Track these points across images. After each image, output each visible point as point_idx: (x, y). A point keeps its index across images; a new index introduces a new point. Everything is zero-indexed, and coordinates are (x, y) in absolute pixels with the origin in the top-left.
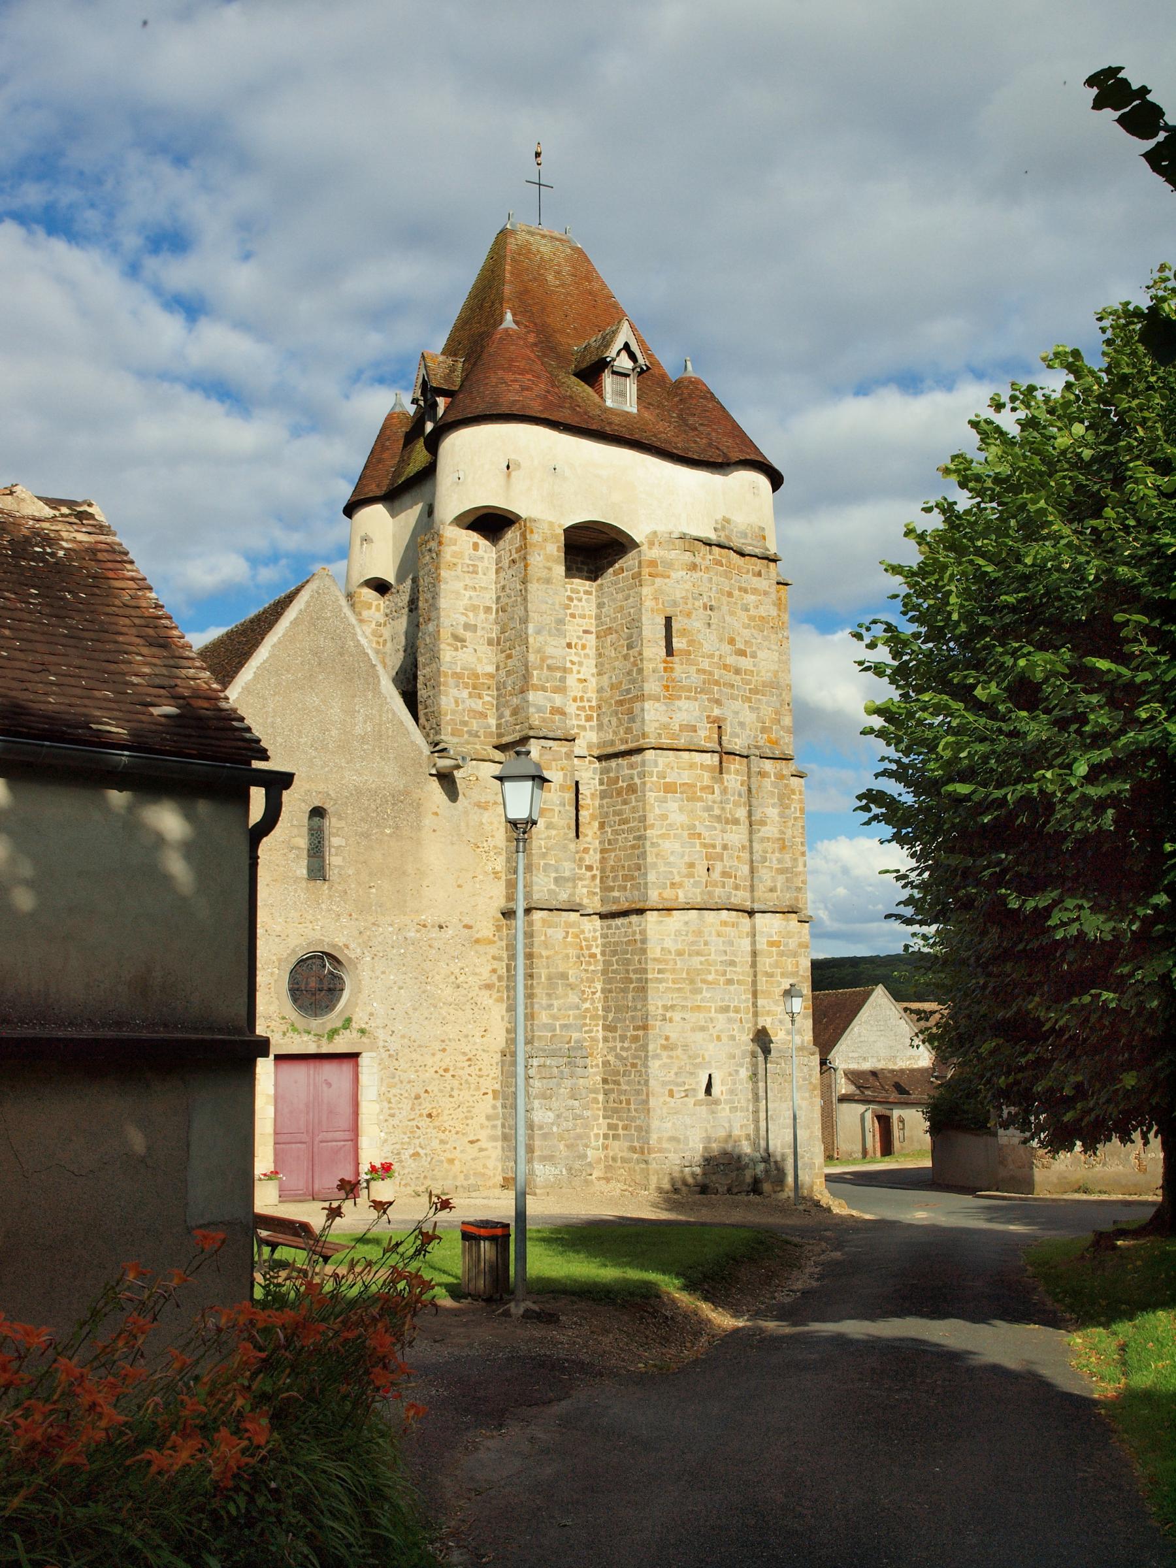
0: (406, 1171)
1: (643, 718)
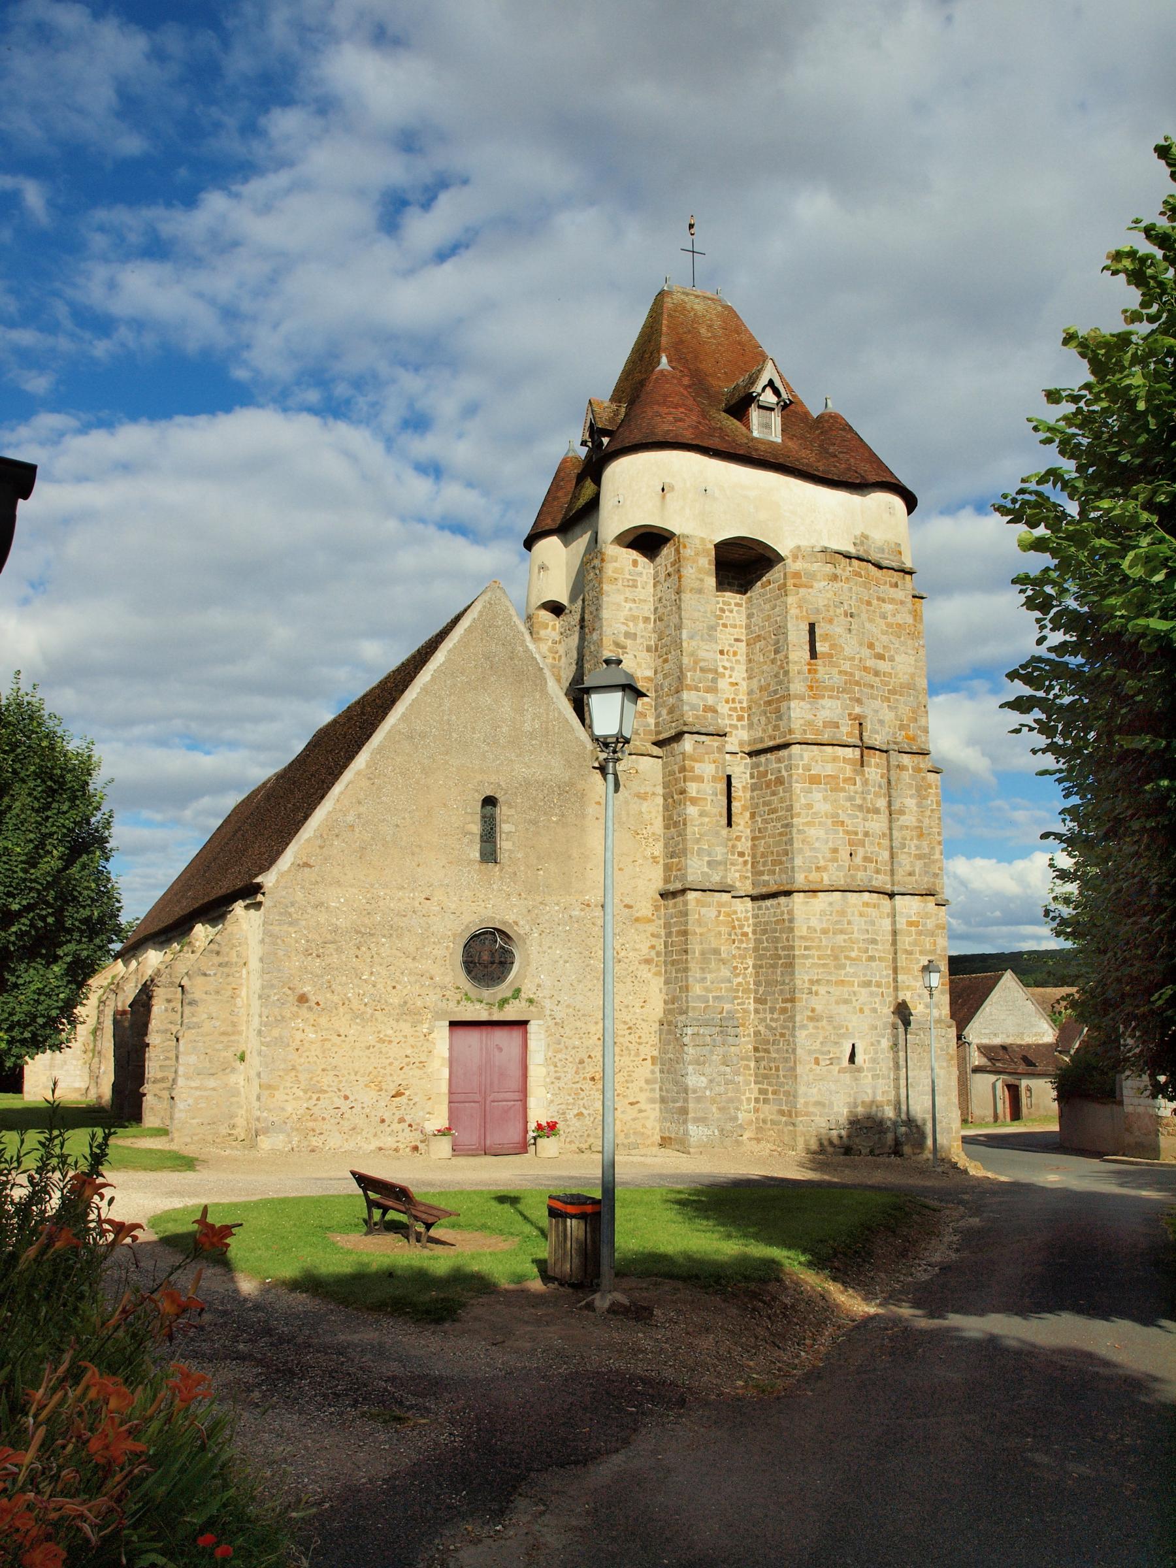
0: (571, 1129)
1: (790, 716)
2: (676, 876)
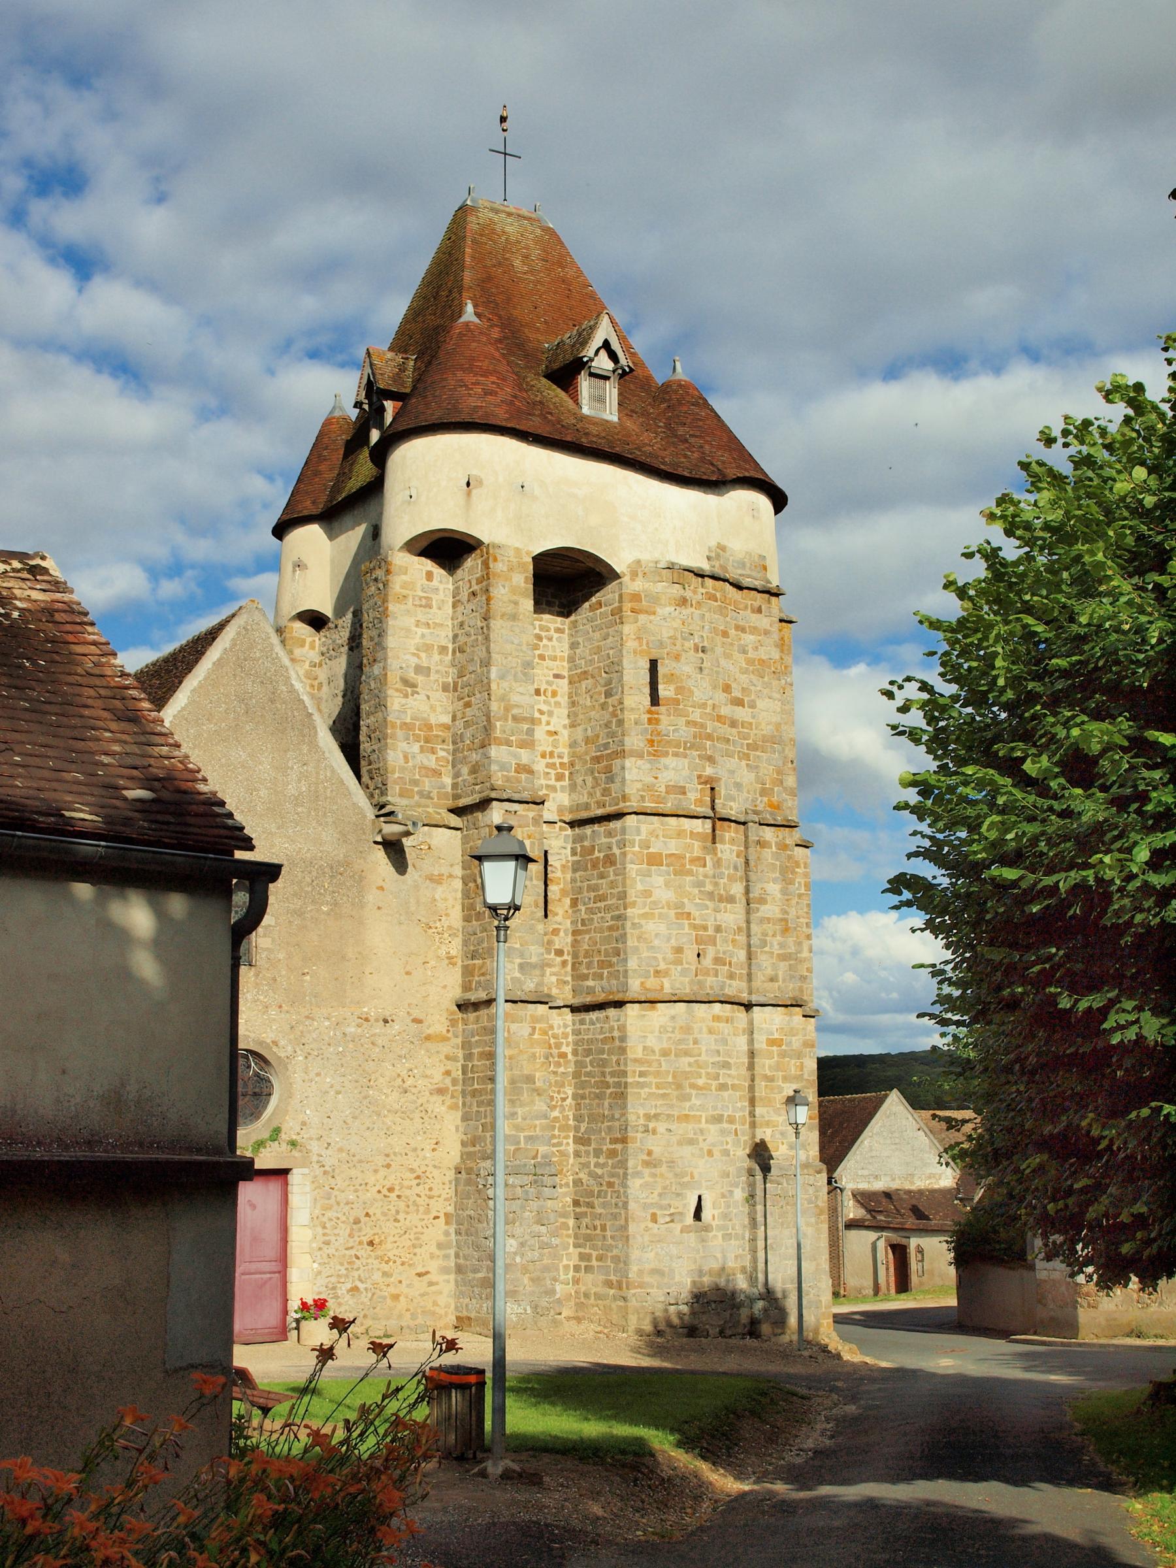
1: (624, 779)
2: (479, 982)
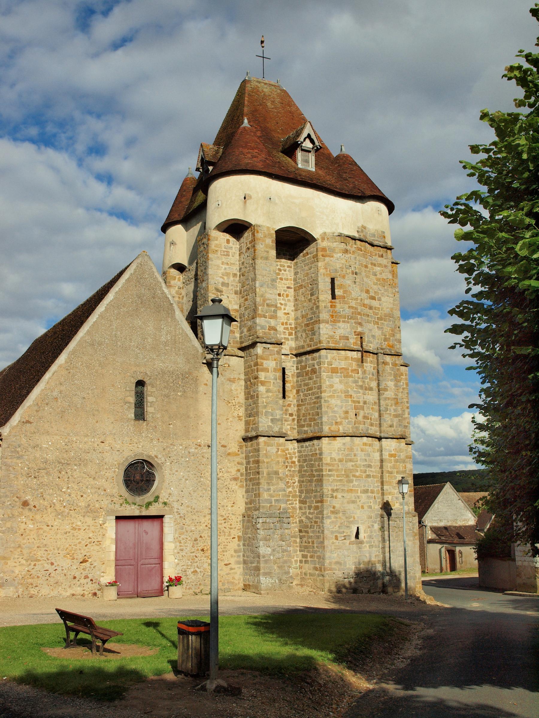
0: (189, 581)
2: (252, 428)
